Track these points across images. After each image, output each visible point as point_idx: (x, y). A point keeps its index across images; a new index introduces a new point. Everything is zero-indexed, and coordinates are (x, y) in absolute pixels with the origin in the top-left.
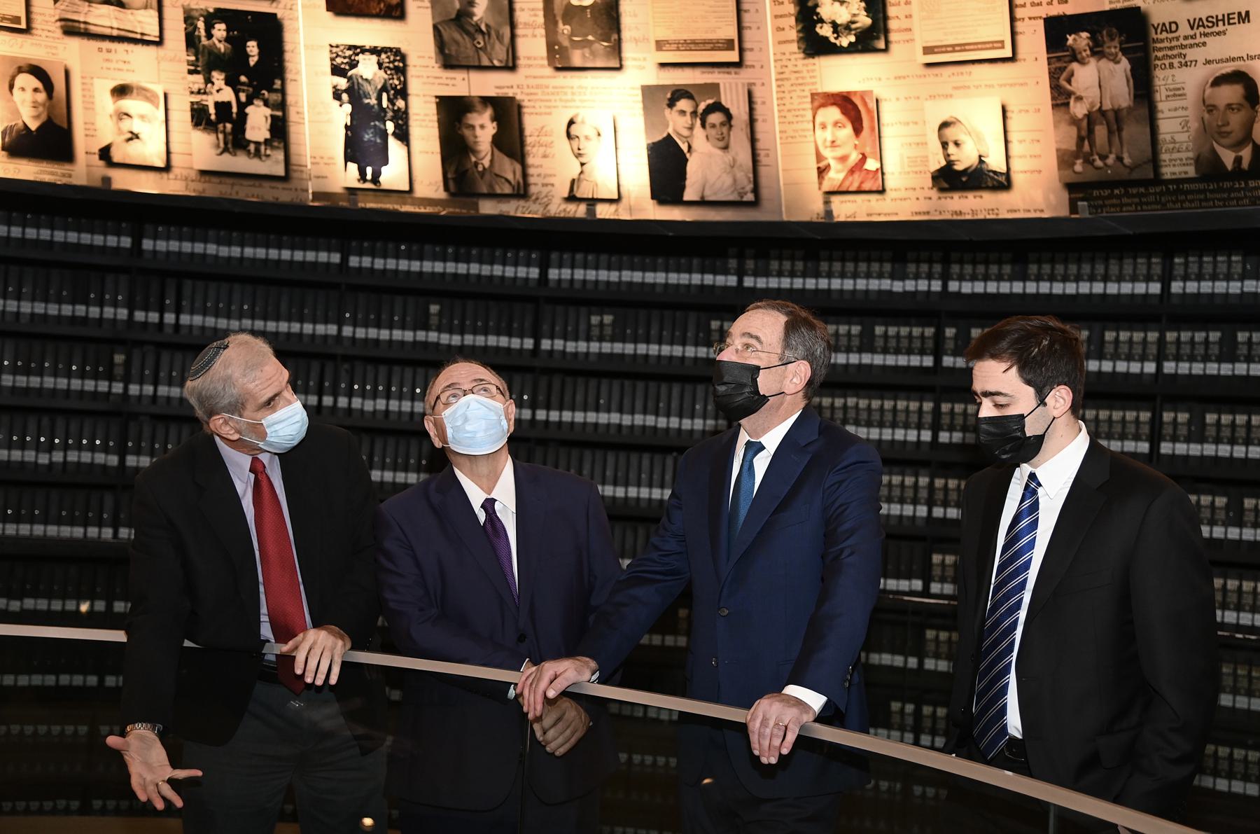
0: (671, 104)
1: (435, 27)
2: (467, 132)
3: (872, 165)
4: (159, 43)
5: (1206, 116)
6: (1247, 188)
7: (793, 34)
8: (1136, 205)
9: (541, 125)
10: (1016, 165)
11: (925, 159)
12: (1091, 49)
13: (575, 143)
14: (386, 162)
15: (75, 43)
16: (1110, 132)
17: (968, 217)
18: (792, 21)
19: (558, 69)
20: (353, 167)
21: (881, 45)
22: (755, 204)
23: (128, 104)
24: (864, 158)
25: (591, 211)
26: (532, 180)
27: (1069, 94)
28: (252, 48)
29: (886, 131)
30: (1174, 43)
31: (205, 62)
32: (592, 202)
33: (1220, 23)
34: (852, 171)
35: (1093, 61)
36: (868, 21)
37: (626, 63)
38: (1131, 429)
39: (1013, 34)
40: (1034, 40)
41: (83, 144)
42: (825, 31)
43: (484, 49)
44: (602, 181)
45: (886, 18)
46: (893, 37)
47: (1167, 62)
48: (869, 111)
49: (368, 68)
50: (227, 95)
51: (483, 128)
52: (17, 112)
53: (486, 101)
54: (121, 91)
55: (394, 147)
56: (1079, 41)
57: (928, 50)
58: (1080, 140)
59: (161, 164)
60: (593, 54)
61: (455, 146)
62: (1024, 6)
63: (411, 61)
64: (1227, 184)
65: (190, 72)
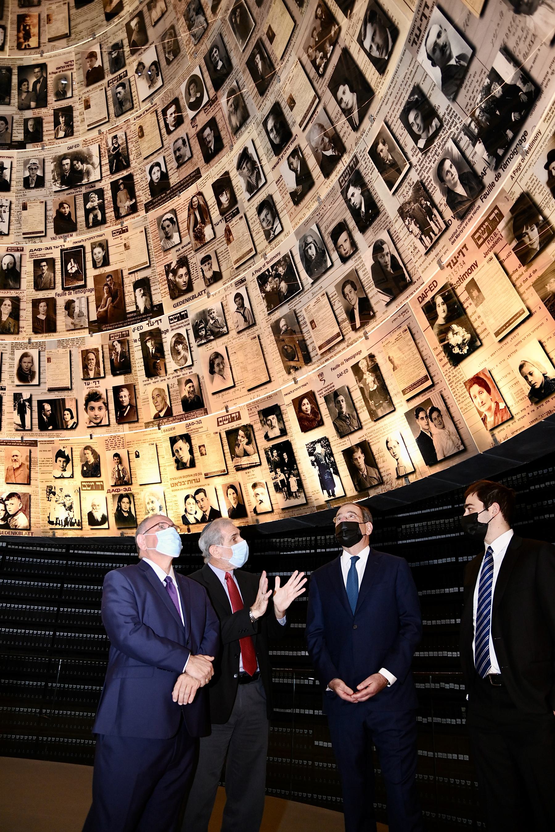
0: (417, 417)
2: (356, 462)
3: (502, 406)
4: (260, 465)
7: (446, 360)
11: (522, 390)
13: (391, 451)
14: (335, 486)
15: (240, 473)
18: (443, 353)
19: (375, 421)
20: (325, 491)
22: (465, 450)
24: (497, 403)
26: (383, 474)
28: (285, 455)
29: (500, 385)
31: (274, 466)
32: (406, 476)
34: (496, 414)
36: (469, 336)
41: (249, 509)
42: (456, 351)
43: (350, 424)
45: (475, 330)
46: (481, 337)
48: (489, 379)
49: (319, 449)
50: (282, 477)
52: (230, 503)
53: (358, 445)
54: (254, 486)
55: (335, 477)
57: (497, 334)
59: (270, 510)
60: (384, 408)
61: (354, 470)
63: (330, 440)
65: (271, 472)
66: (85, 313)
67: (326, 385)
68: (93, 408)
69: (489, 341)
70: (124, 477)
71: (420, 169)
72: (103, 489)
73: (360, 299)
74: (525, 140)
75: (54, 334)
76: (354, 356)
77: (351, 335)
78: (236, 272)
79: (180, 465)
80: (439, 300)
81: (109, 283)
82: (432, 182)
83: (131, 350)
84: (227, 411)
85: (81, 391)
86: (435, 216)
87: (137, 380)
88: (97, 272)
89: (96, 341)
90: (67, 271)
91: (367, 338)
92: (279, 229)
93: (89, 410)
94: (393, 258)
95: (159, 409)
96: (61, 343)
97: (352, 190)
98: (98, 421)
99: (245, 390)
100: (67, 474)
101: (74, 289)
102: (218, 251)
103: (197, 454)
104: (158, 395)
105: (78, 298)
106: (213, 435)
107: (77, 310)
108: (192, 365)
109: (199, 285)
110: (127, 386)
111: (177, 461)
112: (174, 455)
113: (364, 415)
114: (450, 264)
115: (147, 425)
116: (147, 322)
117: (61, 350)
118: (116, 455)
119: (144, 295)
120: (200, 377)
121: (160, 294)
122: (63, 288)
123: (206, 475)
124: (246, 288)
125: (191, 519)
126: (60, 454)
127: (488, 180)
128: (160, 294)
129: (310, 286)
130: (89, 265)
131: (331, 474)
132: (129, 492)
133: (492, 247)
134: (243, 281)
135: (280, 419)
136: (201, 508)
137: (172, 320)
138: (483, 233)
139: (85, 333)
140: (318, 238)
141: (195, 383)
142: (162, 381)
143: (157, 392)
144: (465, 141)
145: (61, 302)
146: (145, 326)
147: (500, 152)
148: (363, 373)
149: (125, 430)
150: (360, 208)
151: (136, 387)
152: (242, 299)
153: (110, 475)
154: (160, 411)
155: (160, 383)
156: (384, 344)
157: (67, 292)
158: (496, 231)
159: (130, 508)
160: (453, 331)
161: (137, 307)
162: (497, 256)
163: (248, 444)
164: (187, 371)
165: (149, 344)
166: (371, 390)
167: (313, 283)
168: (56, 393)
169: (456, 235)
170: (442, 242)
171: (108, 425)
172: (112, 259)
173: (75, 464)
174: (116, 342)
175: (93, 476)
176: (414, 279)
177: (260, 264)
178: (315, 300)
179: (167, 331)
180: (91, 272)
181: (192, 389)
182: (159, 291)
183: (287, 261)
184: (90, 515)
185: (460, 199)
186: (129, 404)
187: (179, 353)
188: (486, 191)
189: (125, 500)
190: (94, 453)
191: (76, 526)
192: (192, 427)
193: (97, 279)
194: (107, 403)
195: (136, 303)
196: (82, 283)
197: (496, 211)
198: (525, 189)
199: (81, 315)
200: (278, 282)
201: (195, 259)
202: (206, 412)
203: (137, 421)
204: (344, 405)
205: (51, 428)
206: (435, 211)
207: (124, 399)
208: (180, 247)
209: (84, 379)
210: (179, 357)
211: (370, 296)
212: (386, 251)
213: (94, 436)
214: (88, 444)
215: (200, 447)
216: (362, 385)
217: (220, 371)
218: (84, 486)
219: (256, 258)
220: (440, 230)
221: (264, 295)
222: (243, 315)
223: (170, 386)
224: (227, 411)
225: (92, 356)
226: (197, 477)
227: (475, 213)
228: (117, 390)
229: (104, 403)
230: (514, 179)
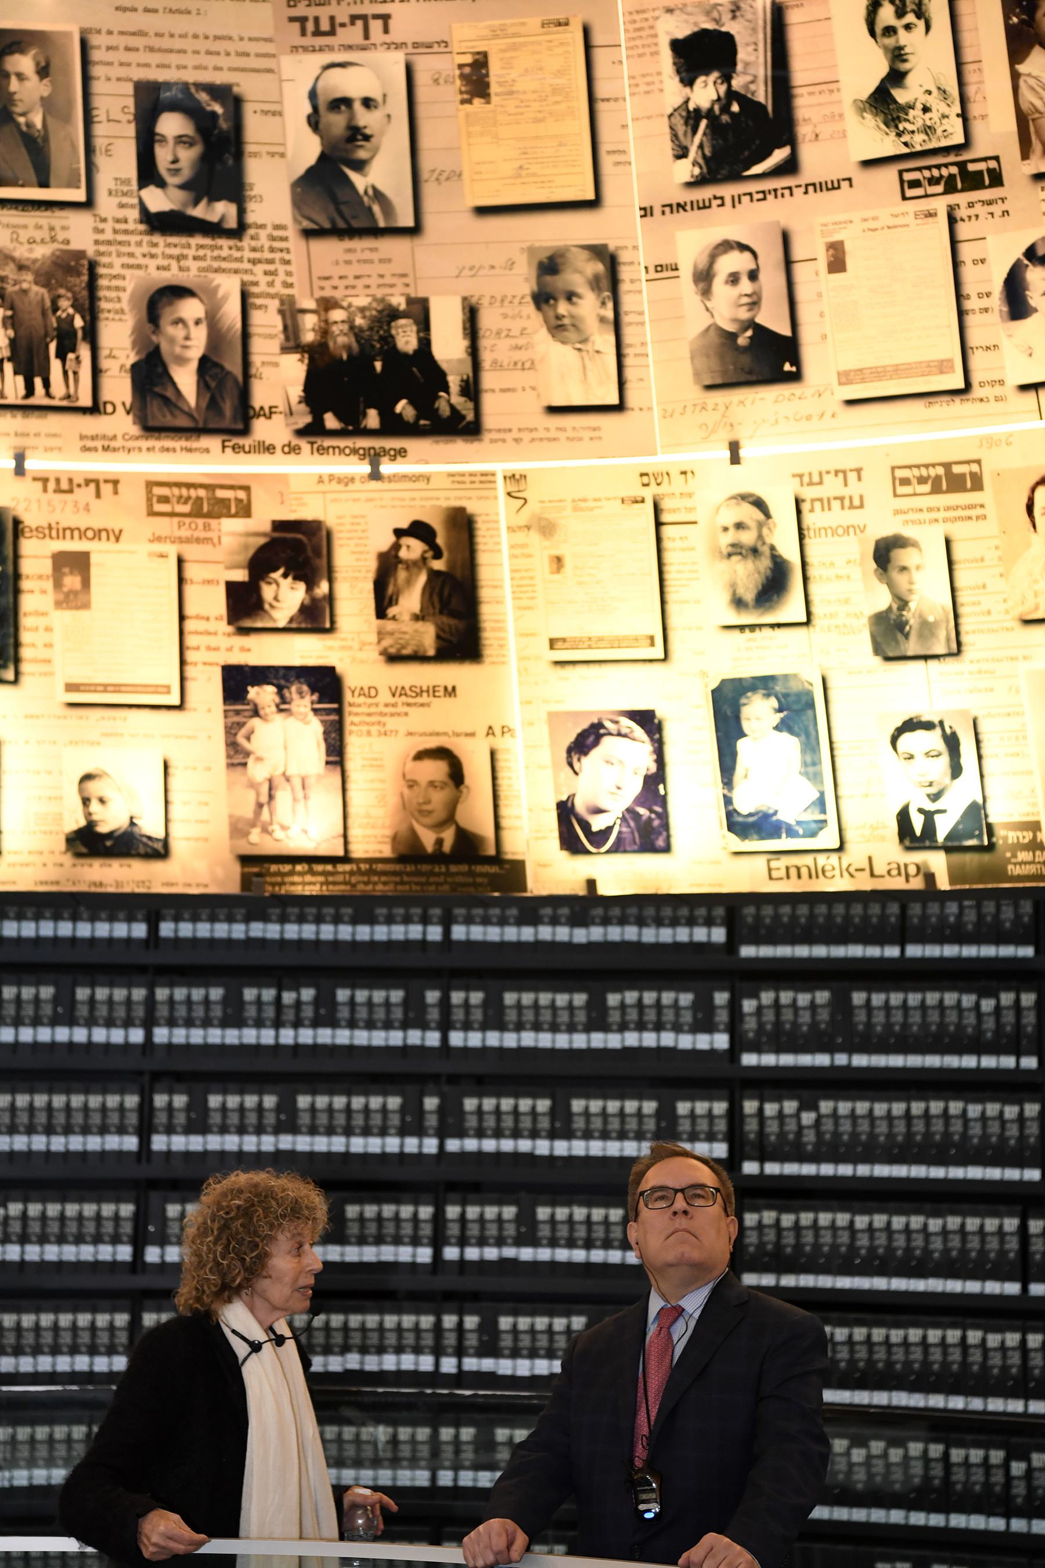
5: (406, 791)
6: (448, 874)
8: (322, 884)
12: (277, 706)
17: (111, 890)
21: (10, 675)
27: (248, 754)
30: (373, 710)
33: (425, 694)
35: (279, 718)
38: (114, 1119)
39: (183, 679)
40: (207, 689)
47: (365, 728)
56: (264, 695)
58: (260, 806)
62: (198, 648)
64: (425, 868)
82: (125, 296)
86: (78, 359)
114: (45, 481)
127: (261, 429)
138: (183, 500)
144: (267, 321)
147: (331, 421)
158: (214, 522)
162: (180, 561)
170: (54, 422)
185: (170, 393)
206: (84, 351)
220: (68, 397)
227: (189, 450)
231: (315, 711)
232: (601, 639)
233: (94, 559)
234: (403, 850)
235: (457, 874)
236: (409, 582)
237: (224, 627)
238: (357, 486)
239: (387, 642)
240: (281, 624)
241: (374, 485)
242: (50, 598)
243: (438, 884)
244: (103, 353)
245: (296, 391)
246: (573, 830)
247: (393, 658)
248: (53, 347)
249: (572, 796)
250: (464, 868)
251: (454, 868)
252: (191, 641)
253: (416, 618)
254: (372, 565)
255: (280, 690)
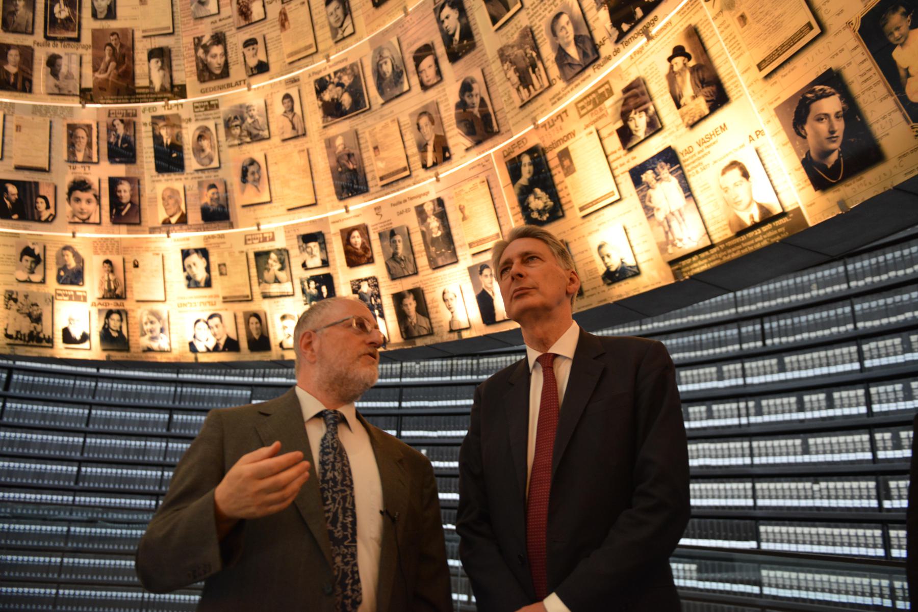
0: (481, 273)
1: (386, 264)
2: (405, 308)
4: (293, 295)
5: (725, 195)
9: (433, 297)
10: (640, 260)
15: (267, 301)
16: (680, 223)
18: (520, 215)
19: (434, 269)
23: (286, 322)
25: (460, 336)
26: (434, 325)
27: (652, 209)
28: (324, 289)
30: (695, 158)
32: (459, 331)
35: (658, 186)
37: (460, 258)
39: (617, 185)
42: (535, 215)
44: (462, 320)
46: (565, 207)
47: (694, 171)
51: (411, 304)
53: (410, 291)
55: (380, 321)
56: (648, 176)
57: (582, 209)
58: (667, 233)
60: (446, 258)
61: (402, 316)
63: (380, 280)
66: (77, 76)
67: (382, 220)
68: (78, 200)
69: (573, 214)
70: (115, 289)
71: (532, 13)
72: (85, 299)
73: (437, 136)
74: (653, 24)
75: (29, 95)
76: (419, 196)
77: (419, 172)
78: (288, 67)
79: (192, 282)
80: (526, 159)
81: (113, 43)
82: (543, 33)
83: (137, 135)
84: (259, 229)
85: (65, 176)
87: (143, 173)
88: (98, 25)
89: (90, 113)
90: (52, 14)
91: (438, 180)
92: (349, 30)
93: (72, 201)
94: (482, 100)
95: (171, 213)
96: (36, 110)
97: (447, 11)
98: (85, 217)
99: (284, 209)
100: (36, 277)
101: (62, 40)
102: (268, 37)
103: (215, 273)
104: (170, 197)
105: (66, 54)
106: (237, 254)
107: (64, 70)
108: (220, 167)
109: (237, 71)
110: (129, 180)
111: (189, 278)
112: (185, 270)
113: (422, 261)
115: (153, 230)
116: (163, 103)
117: (38, 119)
118: (107, 262)
119: (162, 68)
120: (228, 183)
121: (185, 72)
122: (47, 38)
123: (224, 298)
124: (299, 91)
125: (200, 347)
126: (28, 251)
127: (605, 51)
128: (185, 72)
129: (378, 106)
130: (86, 13)
131: (375, 316)
132: (121, 308)
133: (595, 122)
134: (295, 80)
135: (323, 246)
136: (215, 335)
137: (197, 107)
138: (589, 103)
139: (75, 103)
140: (397, 55)
141: (221, 188)
142: (177, 180)
143: (168, 193)
145: (41, 56)
146: (160, 108)
147: (625, 27)
148: (427, 217)
149: (122, 234)
150: (453, 35)
151: (141, 182)
152: (292, 101)
153: (96, 284)
154: (171, 216)
155: (175, 182)
156: (457, 190)
157: (51, 43)
158: (602, 106)
159: (121, 327)
160: (535, 194)
161: (151, 82)
162: (598, 131)
163: (281, 269)
164: (212, 174)
165: (163, 132)
166: (434, 236)
167: (383, 104)
168: (27, 173)
169: (558, 98)
170: (540, 100)
171: (99, 224)
172: (120, 11)
173: (48, 266)
174: (117, 122)
175: (72, 283)
176: (503, 129)
177: (321, 66)
178: (383, 123)
179: (190, 120)
180: (88, 24)
181: (216, 196)
182: (183, 67)
183: (355, 72)
184: (66, 332)
186: (130, 202)
187: (203, 150)
188: (600, 62)
189: (115, 317)
190: (76, 255)
191: (44, 344)
192: (212, 241)
193: (96, 33)
194: (100, 196)
195: (150, 77)
196: (75, 35)
197: (607, 86)
198: (642, 74)
199: (69, 76)
200: (340, 93)
201: (235, 40)
202: (231, 226)
203: (139, 224)
204: (400, 246)
205: (15, 216)
206: (540, 65)
207: (123, 194)
208: (216, 18)
209: (69, 161)
210: (203, 155)
211: (448, 135)
212: (475, 91)
213: (77, 235)
214: (69, 244)
215: (219, 265)
216: (424, 229)
217: (254, 181)
218: (60, 295)
219: (316, 57)
220: (541, 87)
221: (320, 103)
222: (291, 122)
223: (187, 187)
224: (259, 229)
225: (81, 133)
226: (213, 300)
227: (584, 80)
228: (114, 183)
229: (95, 196)
230: (633, 61)
231: (671, 173)
232: (782, 46)
233: (570, 148)
234: (738, 229)
235: (768, 231)
236: (683, 82)
237: (623, 152)
238: (646, 49)
239: (686, 120)
240: (642, 137)
241: (652, 43)
242: (562, 174)
243: (760, 242)
244: (545, 60)
245: (608, 24)
246: (820, 175)
247: (692, 126)
248: (530, 70)
249: (808, 153)
250: (769, 226)
251: (764, 229)
252: (614, 165)
253: (694, 97)
254: (665, 83)
255: (653, 169)
